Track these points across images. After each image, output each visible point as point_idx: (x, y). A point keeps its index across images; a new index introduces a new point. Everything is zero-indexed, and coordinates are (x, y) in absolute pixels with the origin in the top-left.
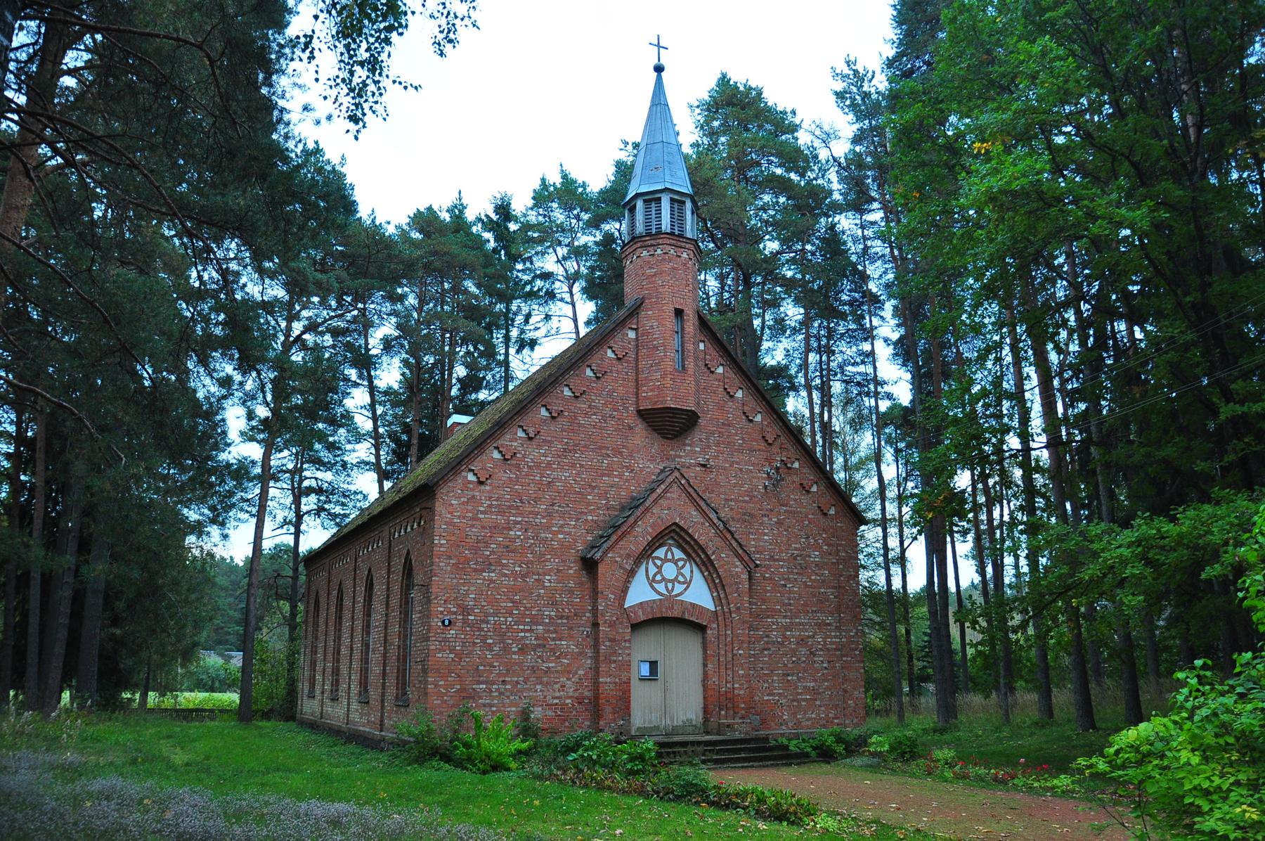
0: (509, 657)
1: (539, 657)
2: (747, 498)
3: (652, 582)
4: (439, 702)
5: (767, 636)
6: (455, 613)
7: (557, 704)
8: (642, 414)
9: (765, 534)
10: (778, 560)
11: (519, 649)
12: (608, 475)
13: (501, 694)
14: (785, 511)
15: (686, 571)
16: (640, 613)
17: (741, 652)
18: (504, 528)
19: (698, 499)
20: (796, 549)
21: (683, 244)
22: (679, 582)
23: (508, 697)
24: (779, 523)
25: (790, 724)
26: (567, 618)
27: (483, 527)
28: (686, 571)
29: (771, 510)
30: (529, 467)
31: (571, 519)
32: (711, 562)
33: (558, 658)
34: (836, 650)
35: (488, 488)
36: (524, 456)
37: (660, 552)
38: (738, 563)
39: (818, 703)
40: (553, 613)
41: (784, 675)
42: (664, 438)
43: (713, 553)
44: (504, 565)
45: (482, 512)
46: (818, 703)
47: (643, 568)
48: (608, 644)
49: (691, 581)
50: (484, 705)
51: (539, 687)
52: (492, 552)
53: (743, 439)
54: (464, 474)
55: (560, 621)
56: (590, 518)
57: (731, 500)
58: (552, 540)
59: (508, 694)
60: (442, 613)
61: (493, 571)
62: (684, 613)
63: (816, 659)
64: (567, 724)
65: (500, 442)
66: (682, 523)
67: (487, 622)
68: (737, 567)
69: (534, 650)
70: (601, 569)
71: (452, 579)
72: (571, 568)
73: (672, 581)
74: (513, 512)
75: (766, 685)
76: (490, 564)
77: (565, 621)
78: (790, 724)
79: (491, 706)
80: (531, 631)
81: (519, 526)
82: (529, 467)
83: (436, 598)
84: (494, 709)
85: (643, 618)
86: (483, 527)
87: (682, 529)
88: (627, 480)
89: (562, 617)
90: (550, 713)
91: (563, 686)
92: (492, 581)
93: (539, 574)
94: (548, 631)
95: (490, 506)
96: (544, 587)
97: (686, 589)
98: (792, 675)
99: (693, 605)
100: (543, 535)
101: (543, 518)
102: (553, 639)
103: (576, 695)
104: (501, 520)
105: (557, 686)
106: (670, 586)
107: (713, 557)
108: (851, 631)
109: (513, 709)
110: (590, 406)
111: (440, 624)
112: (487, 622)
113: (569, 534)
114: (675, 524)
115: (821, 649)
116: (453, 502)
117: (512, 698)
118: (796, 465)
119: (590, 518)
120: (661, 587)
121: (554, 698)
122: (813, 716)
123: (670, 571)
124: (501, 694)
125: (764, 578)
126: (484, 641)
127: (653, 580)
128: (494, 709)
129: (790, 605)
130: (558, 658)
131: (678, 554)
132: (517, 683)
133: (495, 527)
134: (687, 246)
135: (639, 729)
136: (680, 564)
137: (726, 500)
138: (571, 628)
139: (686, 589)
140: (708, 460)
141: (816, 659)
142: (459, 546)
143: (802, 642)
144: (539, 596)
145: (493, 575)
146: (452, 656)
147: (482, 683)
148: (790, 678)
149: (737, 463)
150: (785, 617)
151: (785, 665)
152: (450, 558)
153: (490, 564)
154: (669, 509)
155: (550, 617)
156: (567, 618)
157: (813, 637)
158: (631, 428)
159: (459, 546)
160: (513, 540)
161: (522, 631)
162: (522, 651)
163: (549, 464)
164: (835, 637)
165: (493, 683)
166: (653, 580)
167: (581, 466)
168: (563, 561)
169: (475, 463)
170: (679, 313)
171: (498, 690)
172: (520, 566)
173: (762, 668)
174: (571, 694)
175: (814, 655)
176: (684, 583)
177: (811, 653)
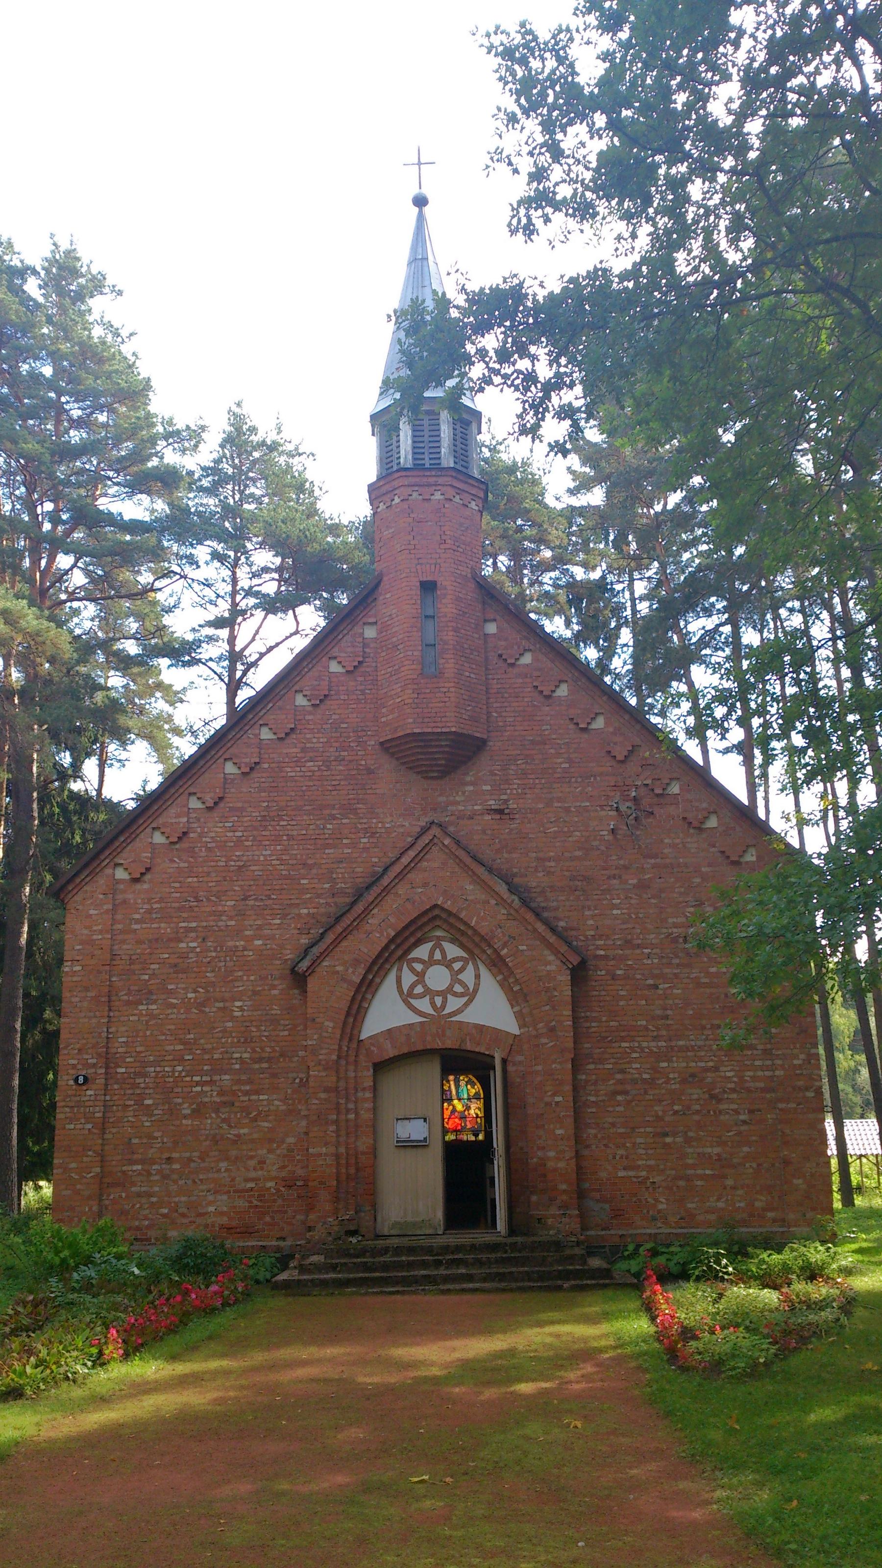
0: (177, 1122)
1: (224, 1120)
2: (579, 853)
3: (407, 997)
4: (68, 1192)
5: (622, 1071)
6: (94, 1066)
7: (252, 1189)
8: (386, 747)
9: (615, 907)
10: (639, 946)
11: (194, 1111)
12: (334, 846)
13: (165, 1177)
14: (654, 866)
15: (468, 976)
16: (388, 1045)
17: (558, 1099)
18: (170, 940)
19: (474, 865)
20: (675, 926)
21: (432, 480)
22: (455, 994)
23: (175, 1182)
24: (642, 886)
25: (672, 1219)
26: (269, 1060)
27: (140, 942)
28: (468, 976)
29: (626, 868)
30: (209, 850)
31: (274, 916)
32: (502, 959)
33: (255, 1119)
34: (764, 1090)
35: (146, 886)
36: (201, 836)
37: (422, 952)
38: (551, 958)
39: (730, 1182)
40: (245, 1055)
41: (656, 1135)
42: (427, 778)
43: (505, 945)
44: (170, 992)
45: (137, 921)
46: (730, 1182)
47: (392, 977)
48: (323, 1095)
49: (476, 991)
50: (139, 1195)
51: (223, 1165)
52: (153, 975)
53: (570, 761)
54: (108, 871)
55: (257, 1066)
56: (305, 911)
57: (549, 860)
58: (245, 949)
59: (175, 1177)
60: (74, 1067)
61: (155, 1002)
62: (463, 1041)
63: (722, 1107)
64: (268, 1219)
65: (161, 820)
66: (448, 905)
67: (145, 1075)
68: (549, 963)
69: (217, 1111)
70: (312, 984)
71: (90, 1018)
72: (274, 987)
73: (443, 994)
74: (185, 915)
75: (621, 1152)
76: (150, 992)
77: (265, 1065)
78: (672, 1219)
79: (150, 1195)
80: (211, 1082)
81: (193, 935)
82: (209, 850)
83: (66, 1048)
84: (154, 1199)
85: (392, 1053)
86: (140, 942)
87: (450, 913)
88: (366, 849)
89: (260, 1060)
90: (242, 1203)
91: (262, 1162)
92: (152, 1016)
93: (223, 1000)
94: (239, 1082)
95: (149, 911)
96: (233, 1018)
97: (466, 1005)
98: (675, 1134)
99: (481, 1028)
100: (230, 944)
101: (231, 918)
102: (247, 1093)
103: (283, 1174)
104: (166, 928)
105: (252, 1163)
106: (438, 1001)
107: (504, 952)
108: (796, 1057)
109: (183, 1199)
110: (304, 750)
111: (72, 1082)
112: (145, 1075)
113: (272, 938)
114: (436, 906)
115: (733, 1090)
116: (92, 912)
117: (181, 1182)
118: (675, 789)
119: (305, 911)
120: (424, 1005)
121: (247, 1180)
122: (721, 1205)
123: (438, 977)
124: (165, 1177)
125: (614, 977)
126: (139, 1102)
127: (410, 994)
128: (154, 1199)
129: (666, 1017)
130: (255, 1119)
131: (453, 951)
132: (190, 1160)
133: (157, 940)
134: (441, 480)
135: (395, 1224)
136: (457, 966)
137: (538, 859)
138: (274, 1075)
139: (466, 1005)
140: (506, 801)
141: (722, 1107)
142: (99, 972)
143: (691, 1078)
144: (224, 1031)
145: (154, 1007)
146: (89, 1126)
147: (136, 1162)
148: (668, 1140)
149: (559, 800)
150: (656, 1038)
151: (659, 1119)
152: (87, 989)
153: (150, 992)
154: (425, 885)
155: (241, 1060)
156: (269, 1060)
157: (716, 1069)
158: (370, 772)
159: (99, 972)
160: (184, 956)
161: (198, 1084)
162: (198, 1112)
163: (239, 842)
164: (762, 1068)
165: (153, 1162)
166: (410, 994)
167: (290, 837)
168: (261, 978)
169: (123, 855)
170: (428, 587)
171: (159, 1172)
172: (195, 991)
173: (613, 1125)
174: (274, 1174)
175: (719, 1101)
176: (462, 995)
177: (712, 1097)
